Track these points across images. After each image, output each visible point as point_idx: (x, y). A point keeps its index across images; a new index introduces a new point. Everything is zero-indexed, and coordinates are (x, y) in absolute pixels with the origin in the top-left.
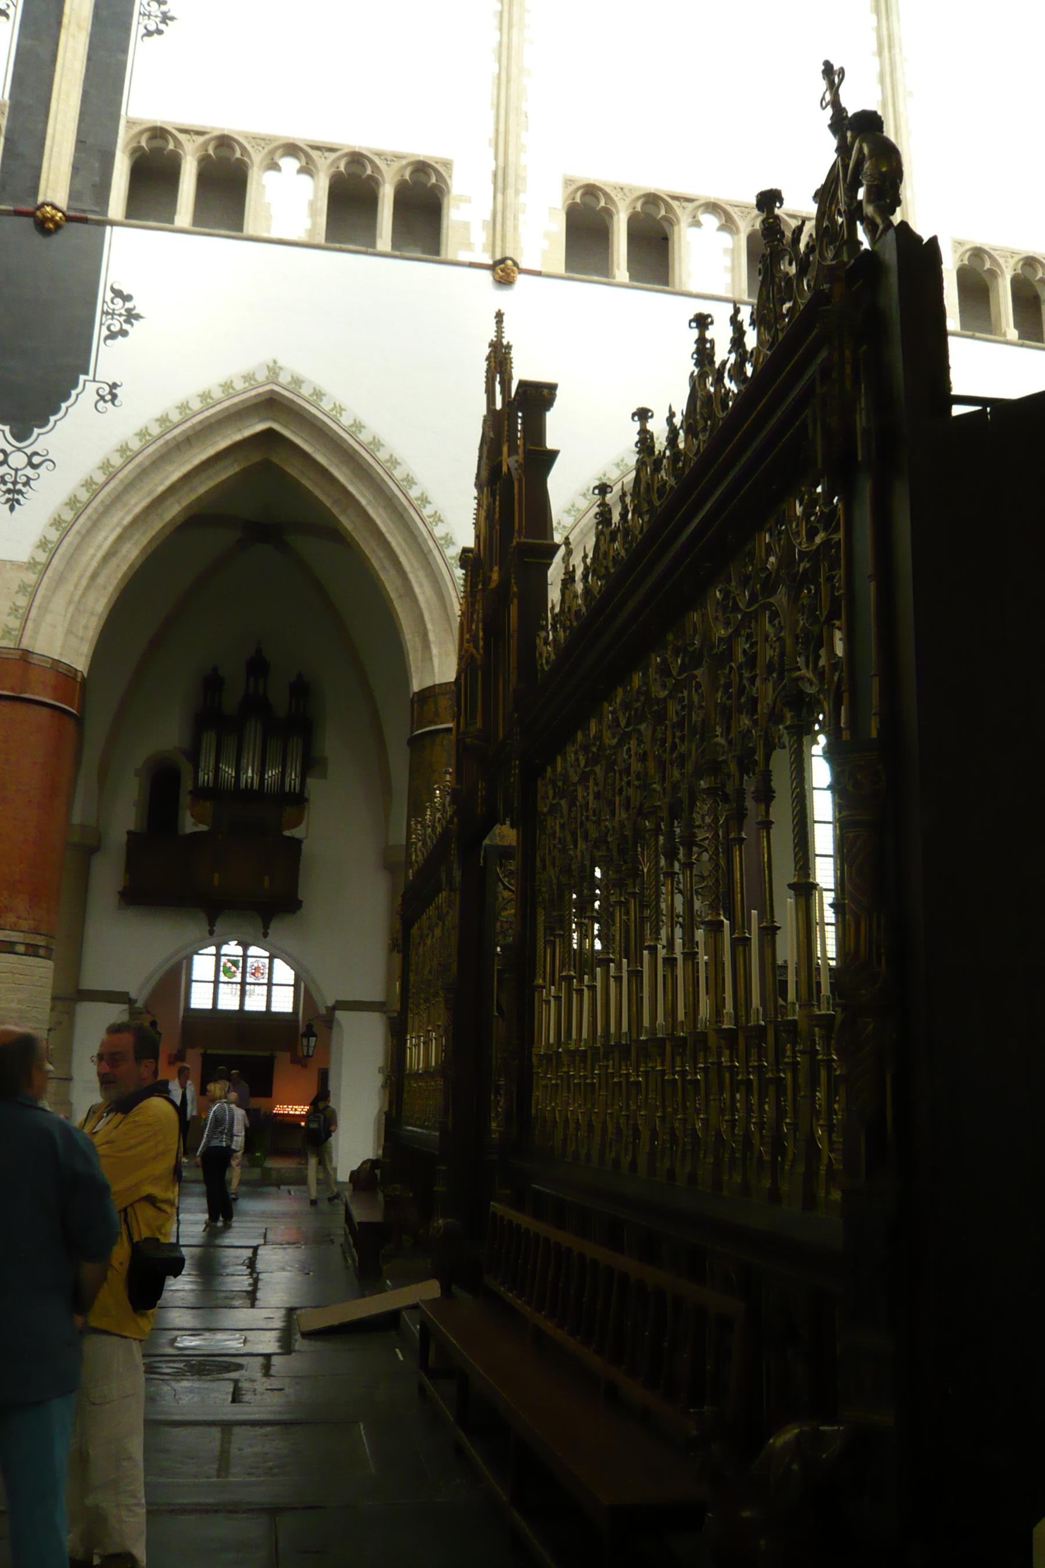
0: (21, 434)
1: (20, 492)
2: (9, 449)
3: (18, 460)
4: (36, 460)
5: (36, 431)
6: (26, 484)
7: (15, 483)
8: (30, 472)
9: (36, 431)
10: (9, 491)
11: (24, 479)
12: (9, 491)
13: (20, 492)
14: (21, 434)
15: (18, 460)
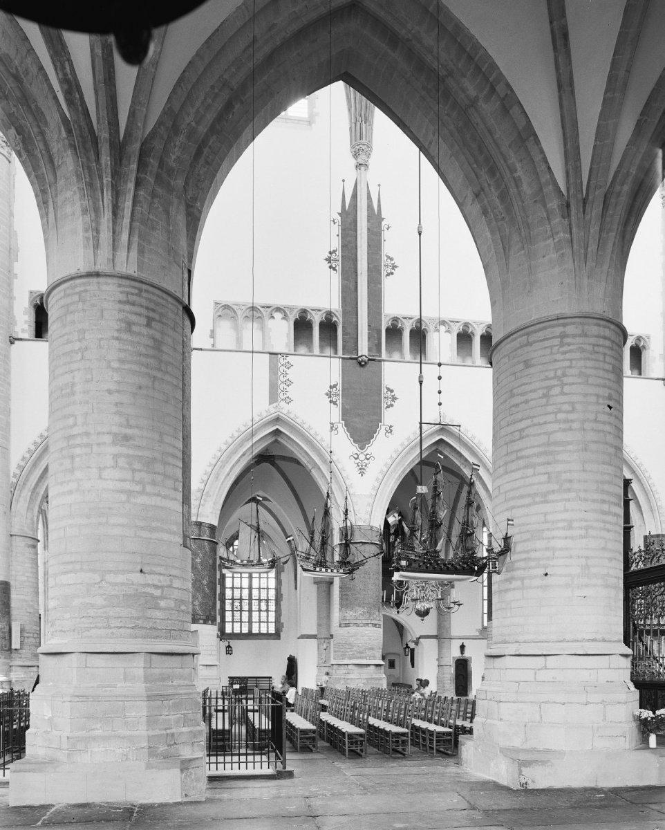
0: (362, 448)
1: (364, 469)
2: (359, 453)
3: (362, 457)
4: (368, 457)
5: (367, 445)
6: (366, 466)
7: (362, 466)
8: (366, 461)
9: (367, 445)
10: (360, 469)
11: (364, 464)
12: (360, 469)
13: (364, 469)
14: (362, 448)
15: (362, 457)
